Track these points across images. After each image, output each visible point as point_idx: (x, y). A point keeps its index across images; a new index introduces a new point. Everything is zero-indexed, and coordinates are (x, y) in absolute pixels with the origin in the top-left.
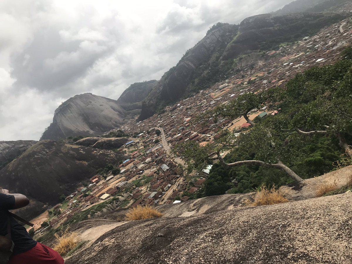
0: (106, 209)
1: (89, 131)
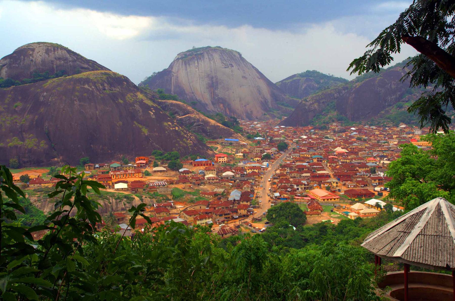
0: (104, 203)
1: (207, 105)
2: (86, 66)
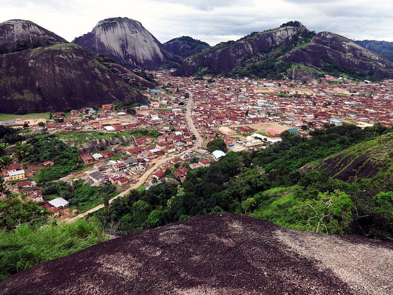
2: (52, 38)
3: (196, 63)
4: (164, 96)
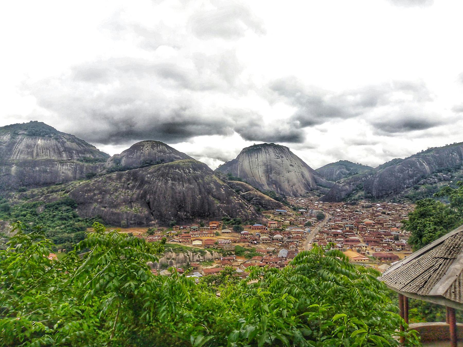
1: (263, 185)
2: (178, 156)
3: (350, 187)
4: (290, 216)
